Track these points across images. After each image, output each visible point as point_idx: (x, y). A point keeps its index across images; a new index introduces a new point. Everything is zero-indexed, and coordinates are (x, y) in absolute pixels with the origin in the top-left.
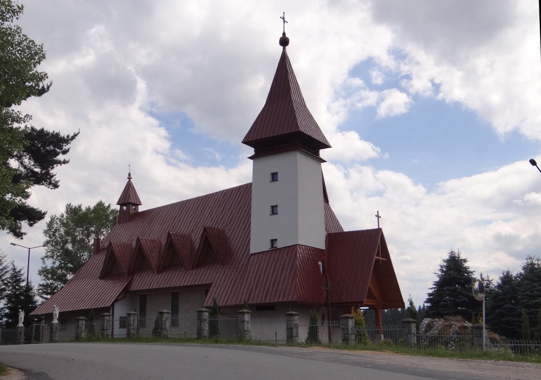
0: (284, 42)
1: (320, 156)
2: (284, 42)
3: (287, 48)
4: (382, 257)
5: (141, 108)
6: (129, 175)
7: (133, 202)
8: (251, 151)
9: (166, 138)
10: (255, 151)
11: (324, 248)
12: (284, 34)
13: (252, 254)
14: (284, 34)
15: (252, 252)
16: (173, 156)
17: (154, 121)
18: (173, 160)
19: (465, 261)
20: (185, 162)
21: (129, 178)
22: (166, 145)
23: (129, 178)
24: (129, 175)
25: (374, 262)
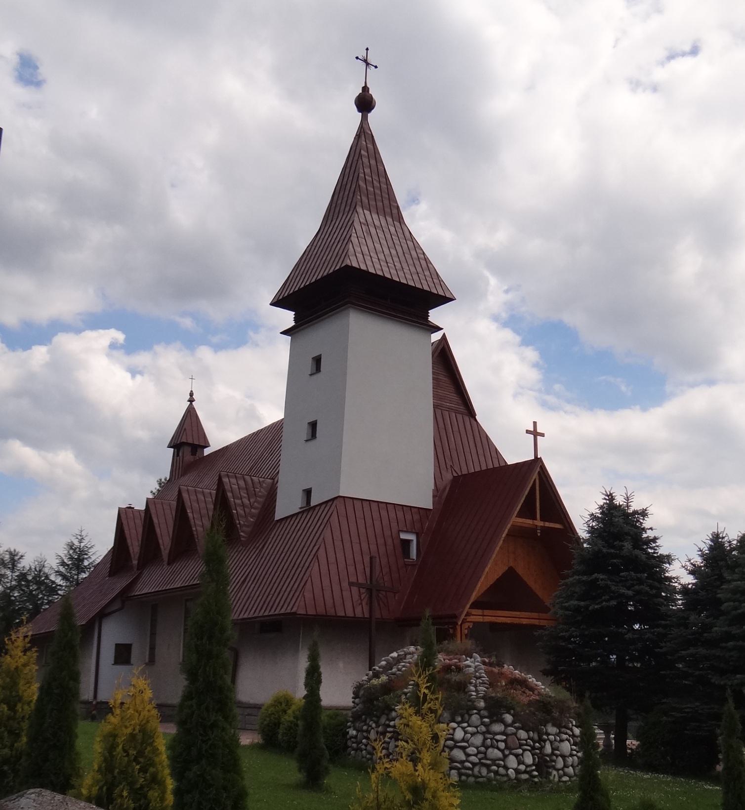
0: (365, 103)
1: (430, 319)
2: (365, 103)
3: (371, 116)
4: (543, 519)
5: (495, 318)
6: (191, 394)
7: (190, 441)
8: (288, 318)
9: (536, 365)
10: (296, 319)
11: (430, 506)
12: (365, 89)
13: (277, 521)
14: (365, 89)
15: (278, 516)
16: (548, 392)
17: (508, 335)
18: (551, 399)
19: (644, 513)
20: (569, 401)
21: (191, 400)
22: (533, 375)
23: (191, 400)
24: (191, 394)
25: (509, 526)
